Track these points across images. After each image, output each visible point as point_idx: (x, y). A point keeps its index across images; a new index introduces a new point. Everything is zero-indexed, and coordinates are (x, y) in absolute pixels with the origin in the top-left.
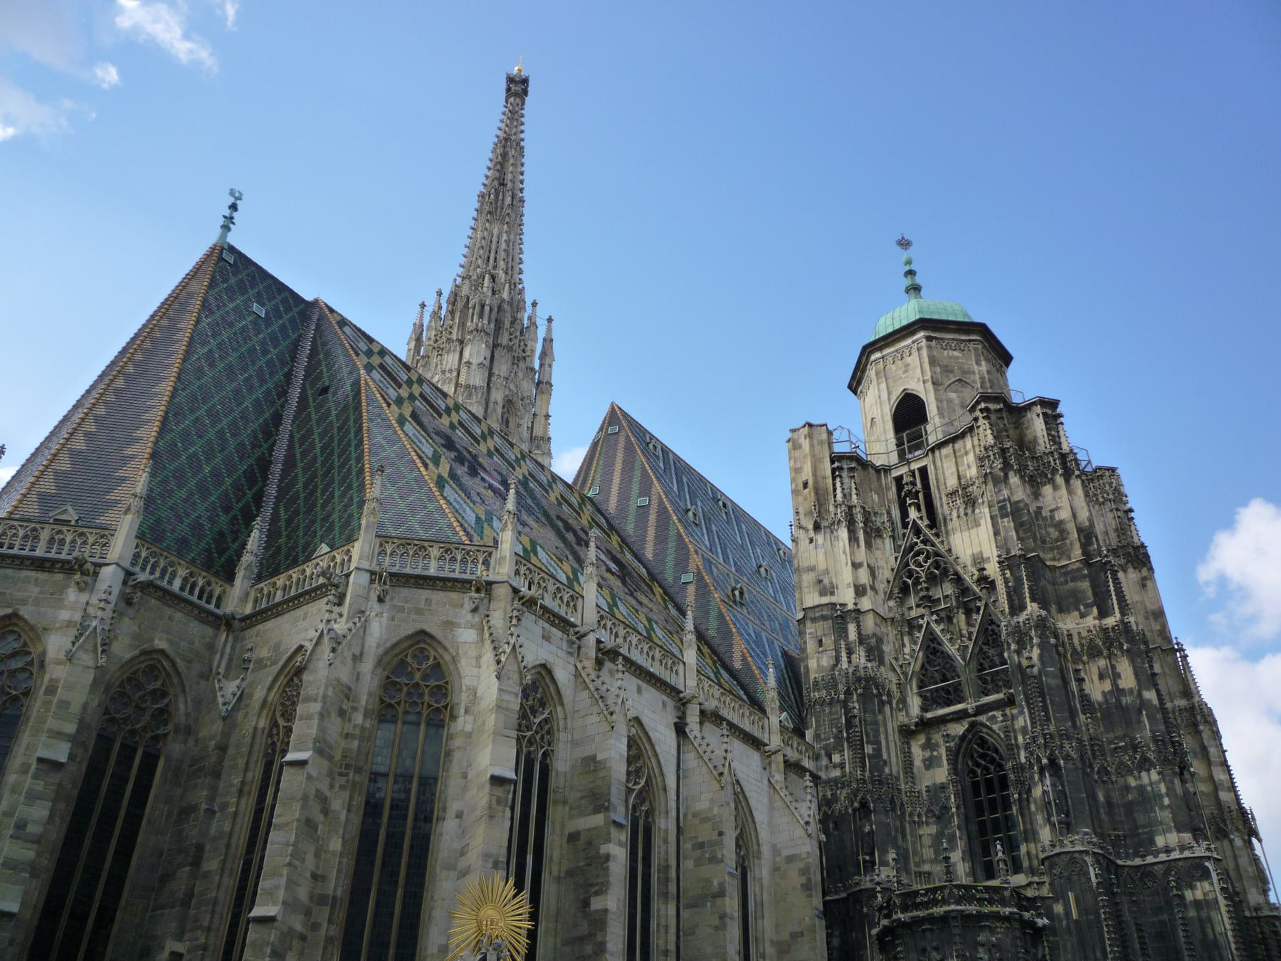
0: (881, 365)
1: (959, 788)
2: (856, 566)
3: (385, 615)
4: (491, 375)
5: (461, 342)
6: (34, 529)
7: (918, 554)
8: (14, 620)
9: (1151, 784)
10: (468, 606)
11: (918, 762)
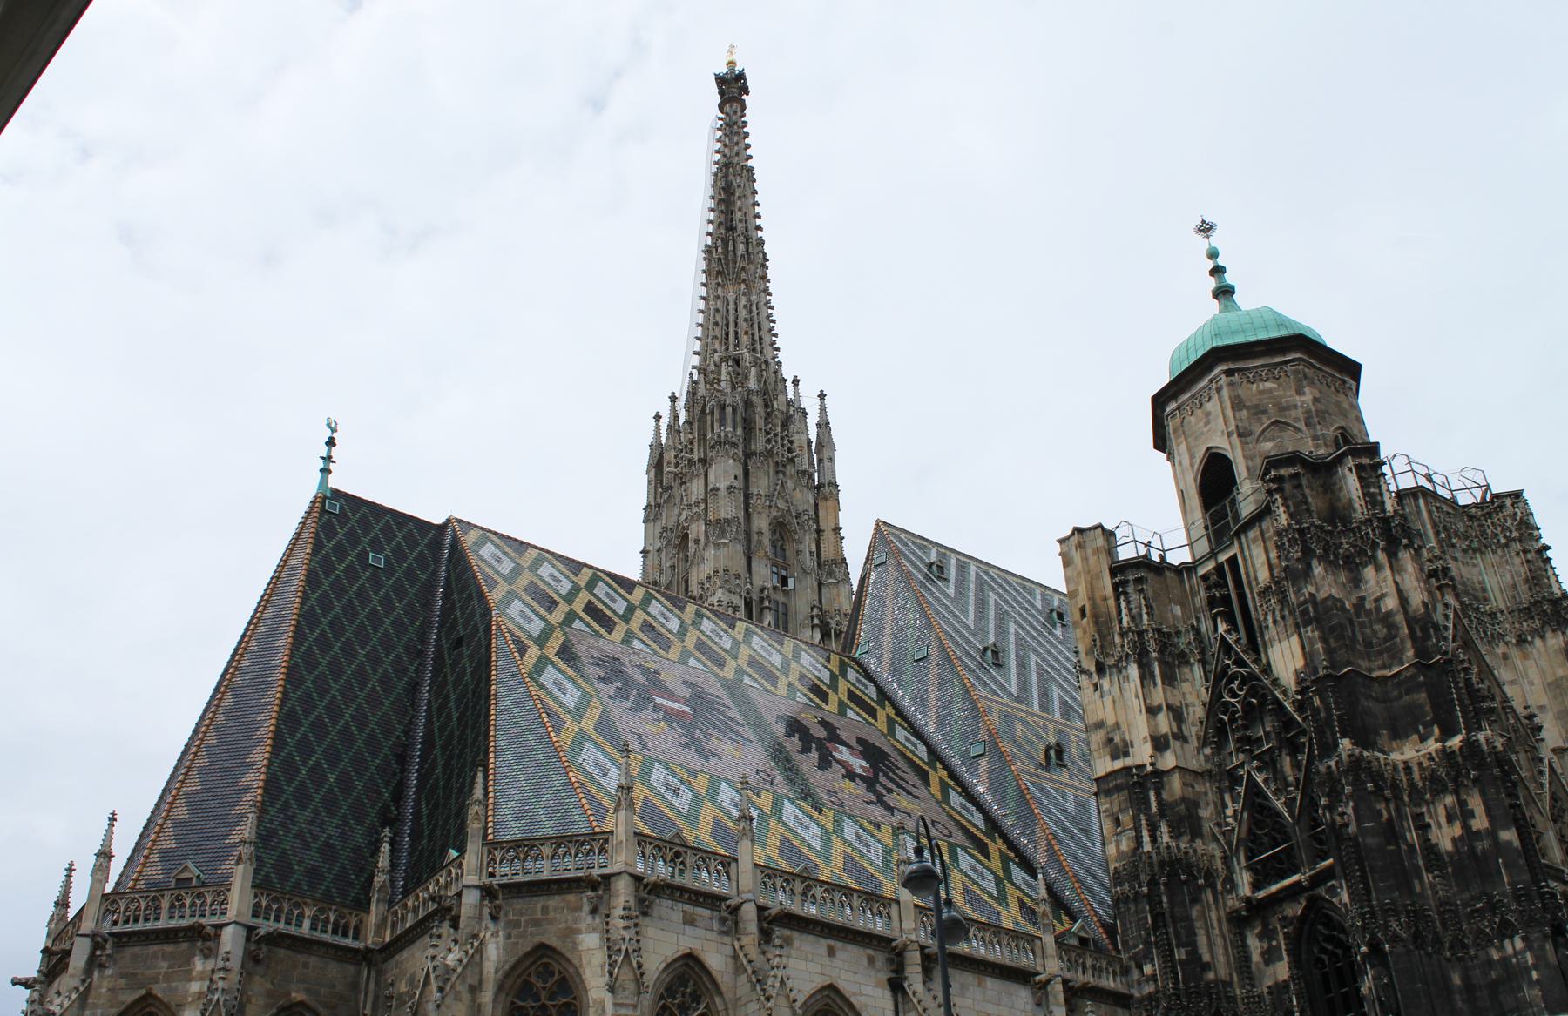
0: (1178, 419)
1: (1303, 985)
2: (1152, 711)
3: (501, 933)
4: (747, 496)
5: (704, 461)
6: (154, 899)
7: (1231, 681)
8: (150, 1001)
9: (1516, 954)
10: (587, 908)
11: (1256, 957)
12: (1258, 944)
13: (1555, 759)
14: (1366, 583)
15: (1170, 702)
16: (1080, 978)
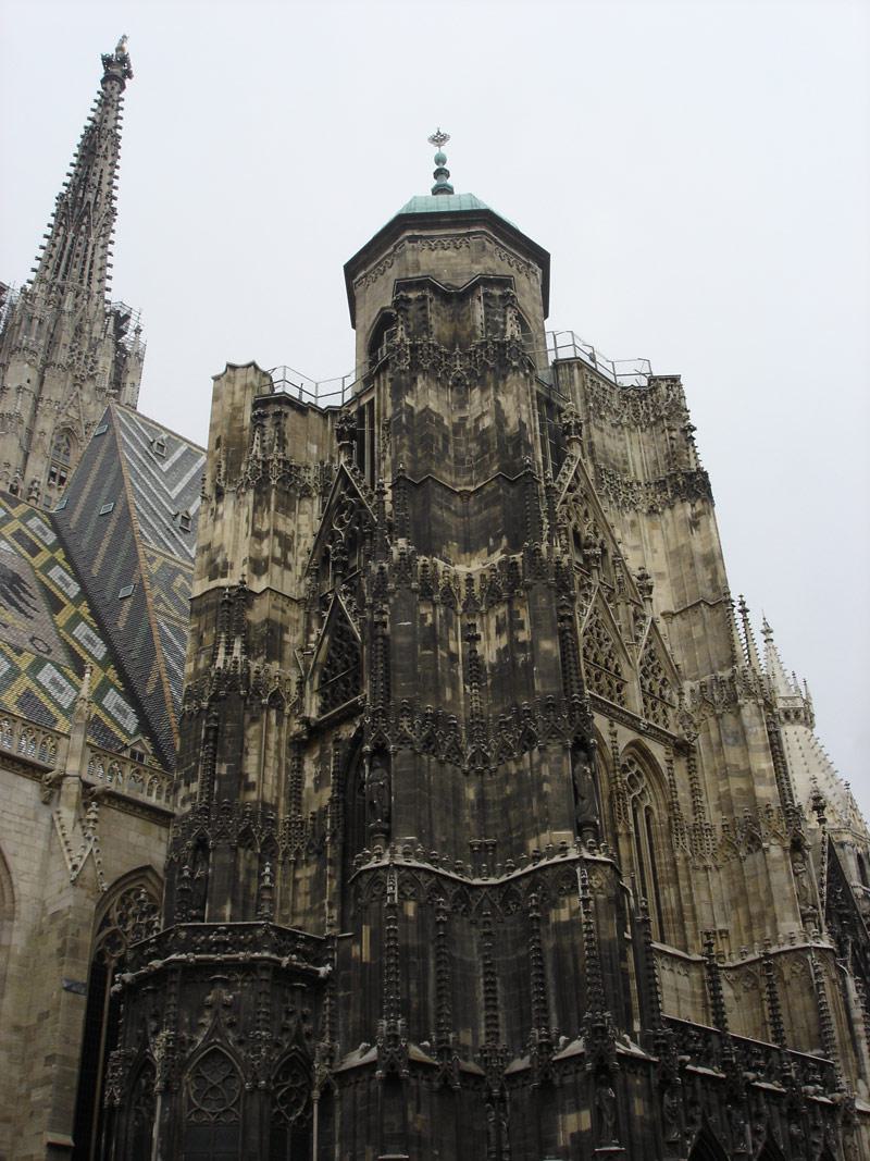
1: (340, 809)
2: (258, 536)
4: (37, 400)
11: (309, 783)
12: (314, 770)
13: (661, 620)
14: (471, 404)
15: (281, 527)
16: (100, 780)
